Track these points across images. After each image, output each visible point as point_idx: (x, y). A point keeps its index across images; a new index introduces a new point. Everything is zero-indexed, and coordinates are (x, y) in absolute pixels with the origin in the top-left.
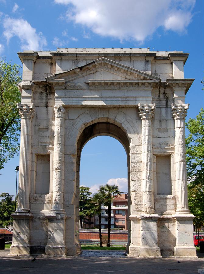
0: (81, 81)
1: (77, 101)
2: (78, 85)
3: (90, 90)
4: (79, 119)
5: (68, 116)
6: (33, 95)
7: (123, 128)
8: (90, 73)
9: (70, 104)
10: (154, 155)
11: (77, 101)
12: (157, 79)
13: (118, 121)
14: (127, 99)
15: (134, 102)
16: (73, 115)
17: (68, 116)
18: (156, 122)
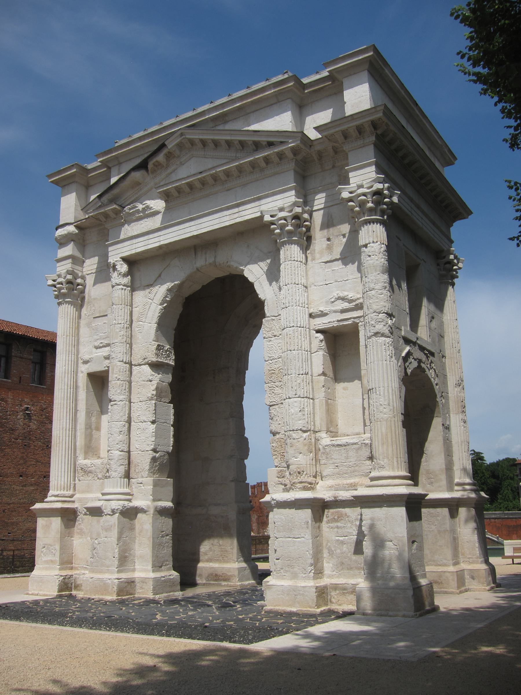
1: (147, 242)
9: (133, 252)
10: (318, 331)
14: (241, 208)
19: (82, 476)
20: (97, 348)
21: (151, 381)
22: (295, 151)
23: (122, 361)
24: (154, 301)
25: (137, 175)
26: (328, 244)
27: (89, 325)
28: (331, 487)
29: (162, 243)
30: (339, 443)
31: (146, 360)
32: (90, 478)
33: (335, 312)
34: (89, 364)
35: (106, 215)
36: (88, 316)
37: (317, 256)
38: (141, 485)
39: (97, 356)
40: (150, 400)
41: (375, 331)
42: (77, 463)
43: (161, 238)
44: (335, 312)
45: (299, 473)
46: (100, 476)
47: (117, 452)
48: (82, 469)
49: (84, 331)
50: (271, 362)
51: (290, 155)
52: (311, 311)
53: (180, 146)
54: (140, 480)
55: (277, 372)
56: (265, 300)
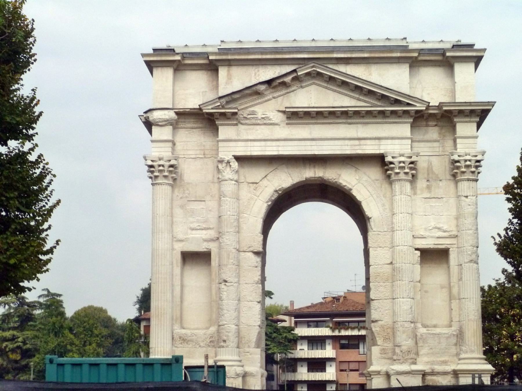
0: (270, 108)
1: (264, 148)
2: (263, 116)
3: (287, 124)
4: (265, 182)
5: (245, 177)
6: (174, 134)
7: (355, 197)
8: (288, 91)
10: (417, 249)
11: (264, 148)
12: (422, 101)
13: (344, 184)
14: (363, 142)
15: (376, 147)
16: (255, 174)
17: (245, 177)
18: (421, 183)
19: (181, 344)
20: (193, 229)
21: (256, 267)
22: (417, 112)
23: (236, 249)
24: (260, 198)
25: (262, 88)
26: (428, 185)
27: (182, 207)
28: (428, 363)
29: (281, 153)
30: (434, 332)
31: (251, 249)
32: (191, 346)
33: (432, 237)
34: (184, 243)
35: (223, 115)
36: (181, 198)
37: (419, 192)
38: (248, 354)
39: (193, 237)
40: (256, 284)
41: (471, 259)
42: (174, 332)
43: (280, 149)
44: (432, 237)
45: (409, 351)
46: (202, 344)
47: (234, 326)
48: (180, 338)
49: (178, 211)
50: (376, 267)
51: (413, 113)
52: (414, 234)
53: (308, 74)
54: (247, 350)
55: (381, 275)
56: (371, 218)
